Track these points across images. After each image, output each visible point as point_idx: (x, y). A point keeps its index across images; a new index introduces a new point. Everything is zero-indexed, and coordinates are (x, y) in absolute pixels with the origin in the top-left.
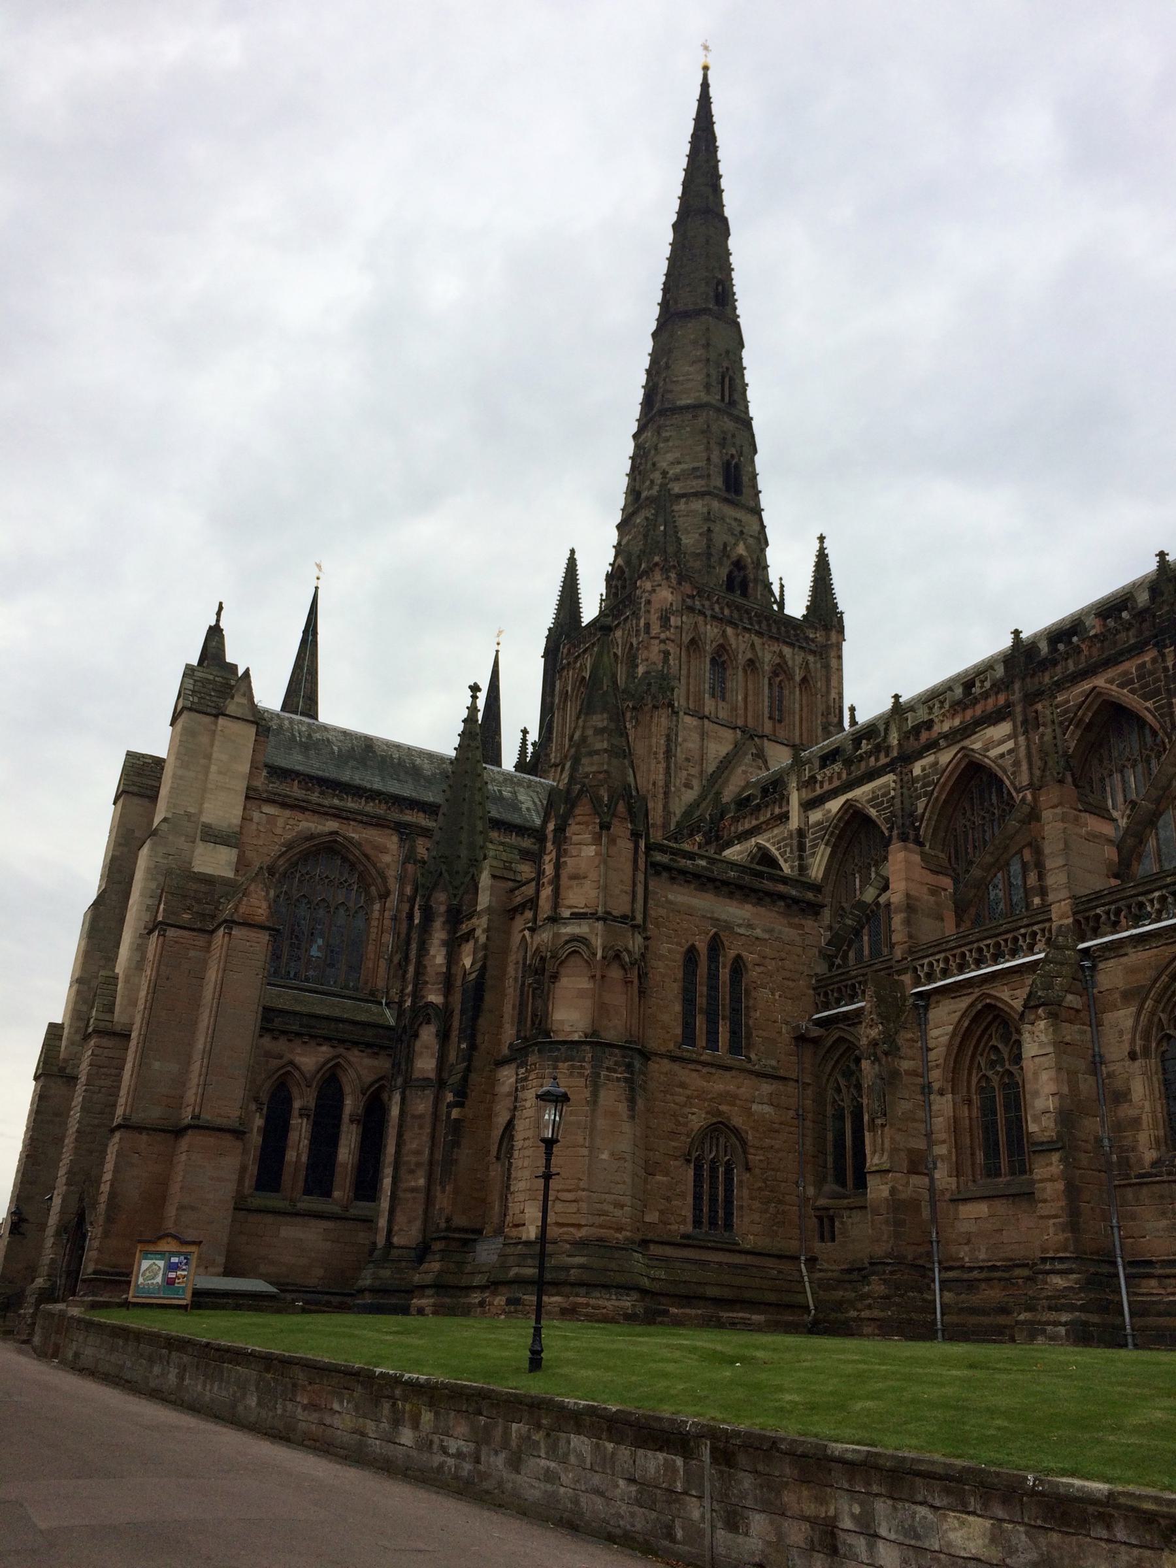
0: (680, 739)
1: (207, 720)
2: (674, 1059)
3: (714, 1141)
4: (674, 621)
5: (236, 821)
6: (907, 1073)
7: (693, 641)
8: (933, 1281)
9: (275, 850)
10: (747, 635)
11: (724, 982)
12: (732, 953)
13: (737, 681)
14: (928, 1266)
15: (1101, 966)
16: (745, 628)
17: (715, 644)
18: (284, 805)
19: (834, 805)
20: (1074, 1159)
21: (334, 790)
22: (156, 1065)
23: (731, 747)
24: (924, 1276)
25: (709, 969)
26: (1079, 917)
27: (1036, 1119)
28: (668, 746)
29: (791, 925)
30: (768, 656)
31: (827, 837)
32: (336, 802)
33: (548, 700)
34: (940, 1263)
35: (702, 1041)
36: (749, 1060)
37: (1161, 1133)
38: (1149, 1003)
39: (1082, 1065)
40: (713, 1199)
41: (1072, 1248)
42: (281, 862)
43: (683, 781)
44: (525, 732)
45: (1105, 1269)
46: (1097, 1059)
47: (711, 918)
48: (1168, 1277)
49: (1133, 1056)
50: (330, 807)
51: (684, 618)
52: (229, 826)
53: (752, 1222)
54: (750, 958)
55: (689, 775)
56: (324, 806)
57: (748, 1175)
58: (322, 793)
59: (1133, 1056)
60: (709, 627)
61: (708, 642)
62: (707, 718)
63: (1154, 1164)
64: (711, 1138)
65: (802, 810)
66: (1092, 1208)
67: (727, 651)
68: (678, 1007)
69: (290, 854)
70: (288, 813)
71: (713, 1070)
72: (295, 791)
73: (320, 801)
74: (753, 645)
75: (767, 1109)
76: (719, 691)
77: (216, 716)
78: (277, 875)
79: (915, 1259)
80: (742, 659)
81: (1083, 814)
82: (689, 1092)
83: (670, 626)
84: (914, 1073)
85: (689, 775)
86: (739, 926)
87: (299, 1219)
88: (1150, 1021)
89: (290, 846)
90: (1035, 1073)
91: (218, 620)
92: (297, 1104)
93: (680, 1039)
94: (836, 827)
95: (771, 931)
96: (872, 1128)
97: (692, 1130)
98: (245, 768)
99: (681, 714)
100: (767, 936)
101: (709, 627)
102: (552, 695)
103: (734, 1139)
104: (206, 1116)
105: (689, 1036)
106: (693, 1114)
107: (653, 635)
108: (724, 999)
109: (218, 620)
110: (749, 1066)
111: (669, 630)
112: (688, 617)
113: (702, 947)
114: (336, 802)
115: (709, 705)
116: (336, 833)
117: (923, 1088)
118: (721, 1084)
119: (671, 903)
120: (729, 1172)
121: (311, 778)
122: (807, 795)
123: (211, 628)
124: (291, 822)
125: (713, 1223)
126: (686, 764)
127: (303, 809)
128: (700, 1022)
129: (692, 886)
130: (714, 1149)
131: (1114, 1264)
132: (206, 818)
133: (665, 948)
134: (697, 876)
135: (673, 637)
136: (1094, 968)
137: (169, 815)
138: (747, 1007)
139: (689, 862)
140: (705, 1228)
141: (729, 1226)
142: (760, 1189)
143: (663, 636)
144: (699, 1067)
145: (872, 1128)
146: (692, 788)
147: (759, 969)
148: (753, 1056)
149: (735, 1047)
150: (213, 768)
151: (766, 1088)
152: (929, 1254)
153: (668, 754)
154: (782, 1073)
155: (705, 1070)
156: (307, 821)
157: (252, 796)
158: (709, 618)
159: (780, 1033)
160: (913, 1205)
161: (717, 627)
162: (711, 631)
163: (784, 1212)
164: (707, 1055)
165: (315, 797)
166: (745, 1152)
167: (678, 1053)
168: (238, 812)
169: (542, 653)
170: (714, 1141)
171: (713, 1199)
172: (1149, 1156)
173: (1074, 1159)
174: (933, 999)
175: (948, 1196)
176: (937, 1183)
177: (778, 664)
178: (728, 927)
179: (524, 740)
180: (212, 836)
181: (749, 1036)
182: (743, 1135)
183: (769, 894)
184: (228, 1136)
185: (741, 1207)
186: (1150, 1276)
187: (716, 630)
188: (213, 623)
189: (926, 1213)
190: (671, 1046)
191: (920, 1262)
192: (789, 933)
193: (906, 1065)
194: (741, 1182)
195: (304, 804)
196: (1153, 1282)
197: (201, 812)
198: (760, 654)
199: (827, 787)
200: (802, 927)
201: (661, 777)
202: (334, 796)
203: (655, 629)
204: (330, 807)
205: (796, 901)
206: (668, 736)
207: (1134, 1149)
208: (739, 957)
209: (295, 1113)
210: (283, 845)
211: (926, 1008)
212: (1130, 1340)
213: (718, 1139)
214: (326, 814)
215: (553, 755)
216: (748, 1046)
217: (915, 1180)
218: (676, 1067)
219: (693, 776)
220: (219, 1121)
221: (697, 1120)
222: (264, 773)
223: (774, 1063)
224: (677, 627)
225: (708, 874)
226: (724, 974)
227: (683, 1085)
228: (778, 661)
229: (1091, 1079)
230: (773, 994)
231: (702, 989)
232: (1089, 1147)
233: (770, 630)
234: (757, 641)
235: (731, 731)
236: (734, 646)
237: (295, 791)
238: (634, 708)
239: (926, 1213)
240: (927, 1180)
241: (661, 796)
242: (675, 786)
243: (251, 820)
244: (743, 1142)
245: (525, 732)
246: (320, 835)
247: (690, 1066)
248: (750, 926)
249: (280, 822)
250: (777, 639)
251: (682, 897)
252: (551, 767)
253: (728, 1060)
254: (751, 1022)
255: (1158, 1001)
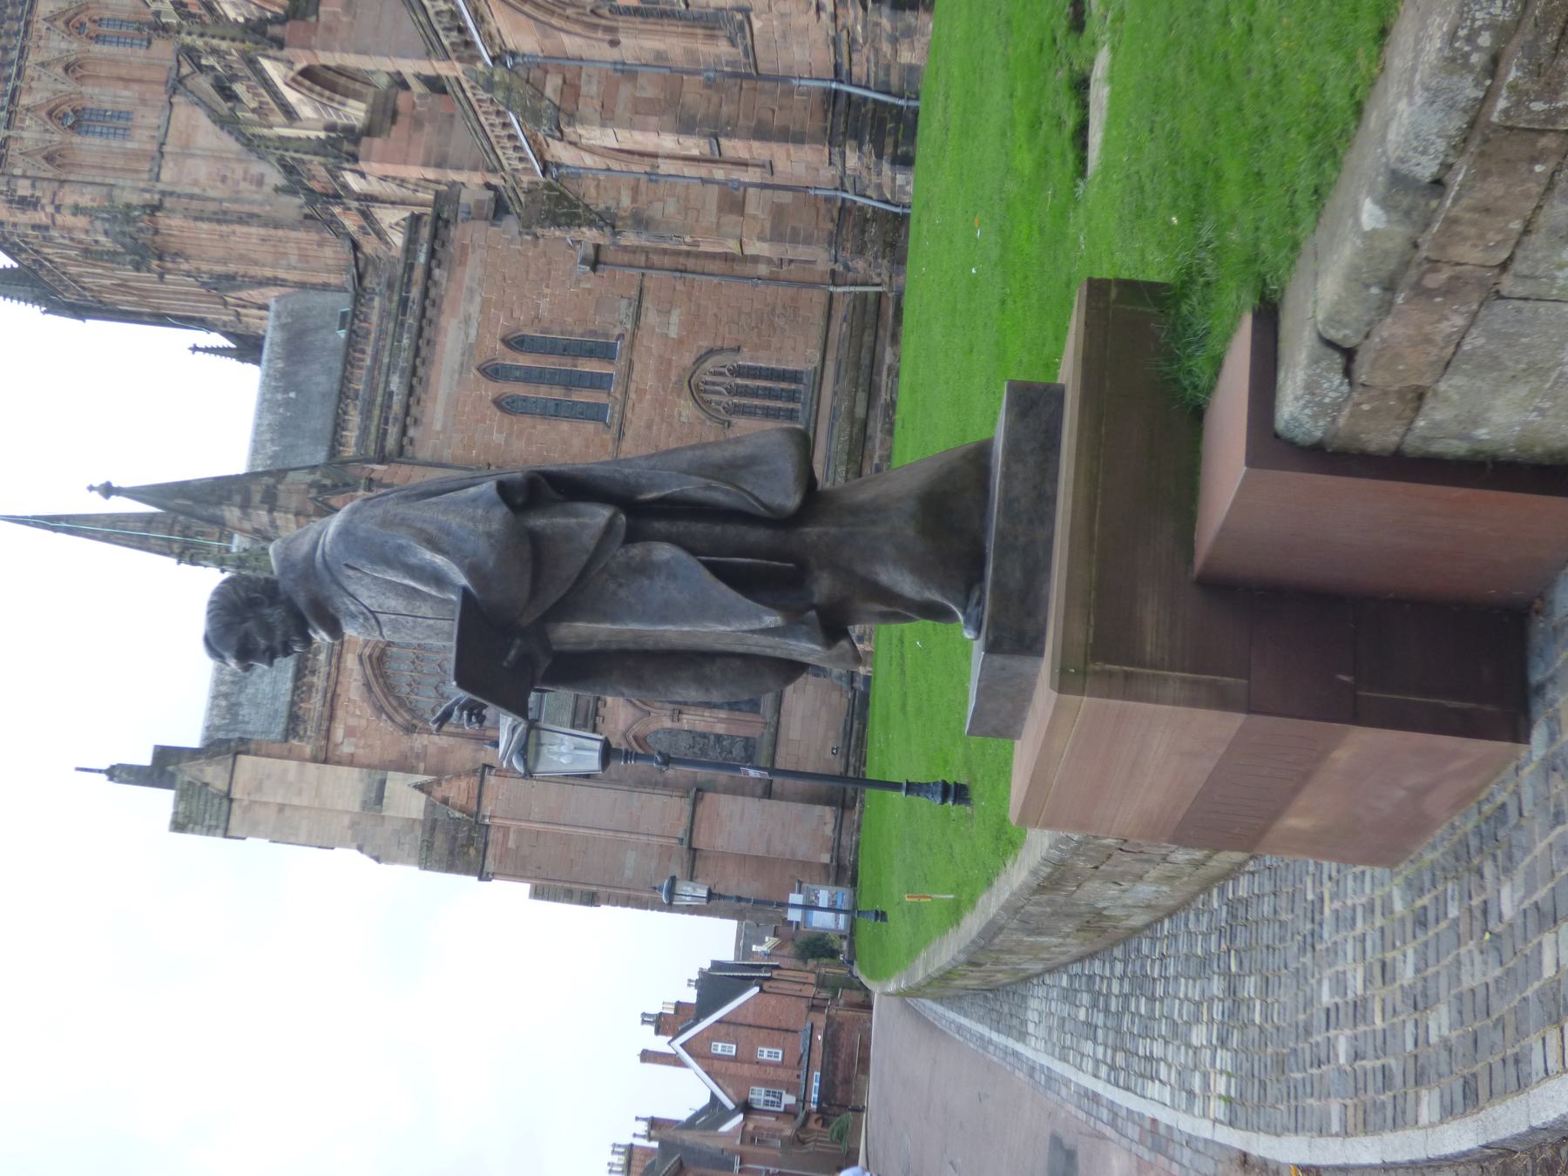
0: (197, 191)
1: (235, 806)
2: (621, 434)
3: (707, 387)
4: (24, 189)
5: (355, 772)
6: (634, 200)
7: (49, 159)
8: (855, 202)
9: (385, 725)
10: (28, 72)
11: (534, 362)
12: (499, 346)
13: (99, 95)
14: (839, 203)
15: (511, 45)
16: (18, 75)
17: (50, 126)
18: (331, 718)
19: (292, 96)
20: (728, 124)
21: (307, 660)
22: (628, 873)
23: (197, 109)
24: (850, 212)
25: (517, 379)
26: (453, 56)
27: (689, 149)
28: (209, 220)
29: (463, 263)
30: (58, 44)
31: (335, 105)
32: (322, 657)
33: (146, 319)
34: (836, 189)
35: (598, 397)
36: (621, 336)
37: (699, 31)
38: (555, 21)
39: (625, 91)
40: (770, 394)
41: (821, 147)
42: (398, 719)
43: (253, 188)
44: (195, 349)
45: (842, 102)
46: (619, 67)
47: (461, 373)
48: (850, 60)
49: (614, 43)
50: (330, 664)
51: (18, 172)
52: (362, 780)
53: (794, 349)
54: (502, 324)
55: (245, 179)
56: (329, 674)
57: (745, 350)
58: (313, 672)
59: (614, 43)
60: (25, 134)
61: (48, 136)
62: (163, 144)
63: (733, 43)
64: (705, 391)
65: (298, 124)
66: (780, 109)
67: (57, 107)
68: (565, 426)
69: (388, 709)
70: (340, 713)
71: (632, 387)
72: (315, 704)
73: (323, 675)
74: (43, 64)
75: (675, 318)
76: (117, 122)
77: (231, 800)
78: (415, 722)
79: (832, 220)
80: (68, 86)
81: (323, 18)
82: (657, 419)
83: (32, 196)
84: (635, 191)
85: (245, 179)
86: (467, 335)
87: (783, 720)
88: (577, 21)
89: (380, 710)
90: (635, 142)
91: (100, 771)
92: (668, 724)
93: (601, 426)
94: (321, 95)
95: (471, 291)
96: (696, 244)
97: (698, 418)
98: (292, 765)
99: (160, 186)
100: (478, 299)
101: (25, 134)
102: (140, 314)
103: (709, 365)
104: (680, 834)
105: (595, 413)
106: (680, 415)
107: (50, 222)
108: (554, 364)
109: (100, 771)
110: (628, 337)
111: (38, 199)
112: (14, 165)
113: (491, 389)
114: (322, 657)
115: (141, 140)
116: (360, 657)
117: (651, 180)
118: (646, 376)
119: (444, 428)
120: (739, 372)
121: (296, 688)
122: (278, 117)
123: (111, 779)
124: (351, 709)
125: (792, 396)
126: (230, 182)
127: (334, 695)
128: (582, 396)
129: (423, 396)
130: (717, 388)
131: (836, 92)
132: (356, 807)
133: (498, 438)
134: (411, 390)
135: (49, 194)
136: (513, 54)
137: (355, 845)
138: (562, 334)
139: (395, 398)
140: (798, 406)
141: (794, 377)
142: (759, 335)
143: (50, 209)
144: (630, 403)
145: (696, 244)
146: (262, 176)
147: (516, 314)
148: (617, 331)
149: (605, 352)
150: (296, 801)
151: (651, 317)
152: (828, 199)
153: (221, 218)
154: (634, 293)
155: (633, 396)
156: (348, 690)
157: (325, 757)
158: (12, 133)
159: (590, 291)
160: (778, 212)
161: (23, 120)
162: (31, 133)
163: (784, 307)
164: (617, 391)
165: (319, 681)
166: (721, 350)
167: (615, 429)
168: (343, 771)
169: (80, 322)
170: (707, 387)
171: (770, 394)
172: (723, 48)
173: (728, 124)
174: (548, 157)
175: (768, 176)
176: (754, 181)
177: (67, 23)
178: (469, 350)
179: (207, 350)
180: (377, 797)
181: (594, 333)
182: (703, 351)
183: (425, 293)
184: (699, 809)
185: (778, 361)
186: (850, 73)
187: (28, 122)
188: (104, 777)
189: (786, 198)
190: (608, 437)
191: (835, 214)
192: (474, 259)
193: (626, 201)
194: (752, 359)
195: (329, 695)
196: (855, 70)
197: (347, 812)
198: (56, 54)
199: (267, 98)
200: (464, 248)
201: (254, 230)
202: (315, 659)
203: (40, 217)
204: (330, 664)
205: (432, 253)
206: (196, 219)
207: (718, 56)
208: (506, 342)
209: (676, 725)
210: (379, 718)
211: (558, 166)
212: (912, 103)
213: (706, 383)
214: (338, 669)
215: (225, 318)
216: (606, 335)
217: (751, 208)
218: (629, 433)
219: (246, 172)
220: (685, 820)
221: (686, 409)
222: (295, 742)
223: (624, 303)
224: (33, 186)
225: (408, 373)
226: (524, 360)
227: (649, 426)
228: (60, 23)
229: (641, 81)
230: (545, 296)
231: (543, 392)
232: (715, 99)
233: (16, 34)
234: (32, 58)
235: (176, 110)
236: (48, 95)
237: (315, 704)
238: (160, 258)
239: (786, 198)
240: (751, 191)
241: (280, 233)
242: (262, 204)
243: (352, 755)
244: (711, 352)
245: (195, 349)
246: (365, 675)
247: (629, 415)
248: (467, 320)
249: (352, 722)
250: (27, 24)
251: (437, 411)
252: (240, 321)
253: (621, 363)
254: (579, 330)
255: (553, 13)
